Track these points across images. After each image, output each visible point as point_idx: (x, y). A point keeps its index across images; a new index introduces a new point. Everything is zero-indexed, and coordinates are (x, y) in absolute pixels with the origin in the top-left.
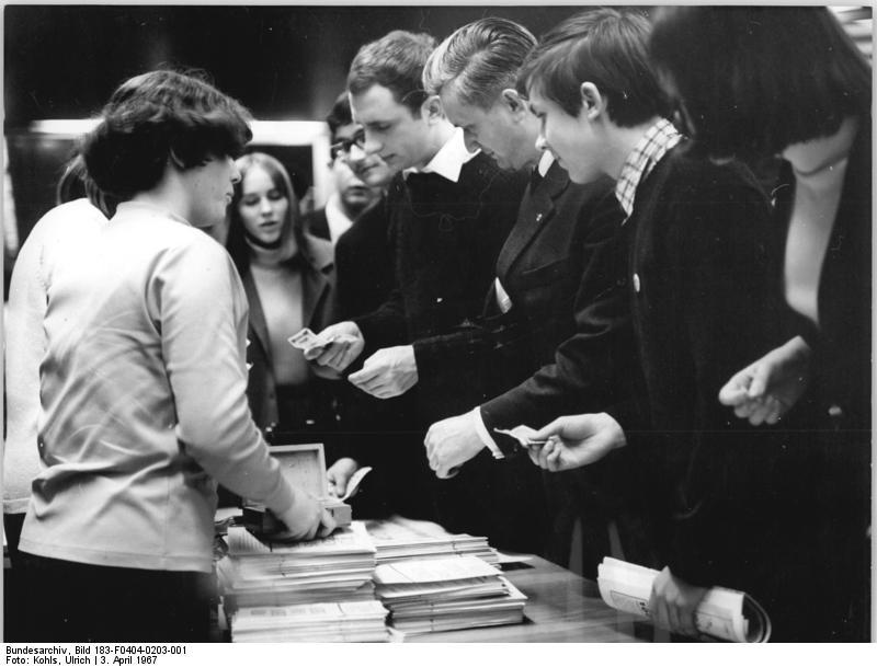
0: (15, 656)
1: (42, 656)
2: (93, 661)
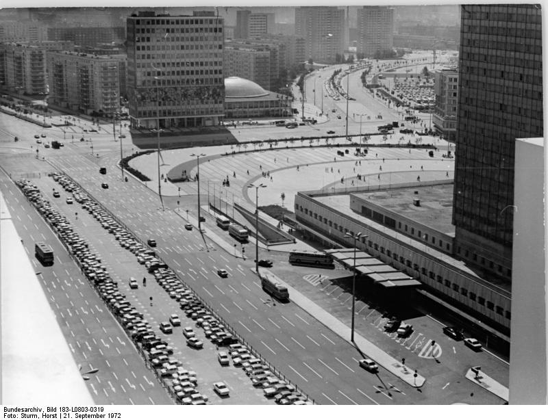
0: (10, 413)
1: (27, 413)
2: (58, 416)
